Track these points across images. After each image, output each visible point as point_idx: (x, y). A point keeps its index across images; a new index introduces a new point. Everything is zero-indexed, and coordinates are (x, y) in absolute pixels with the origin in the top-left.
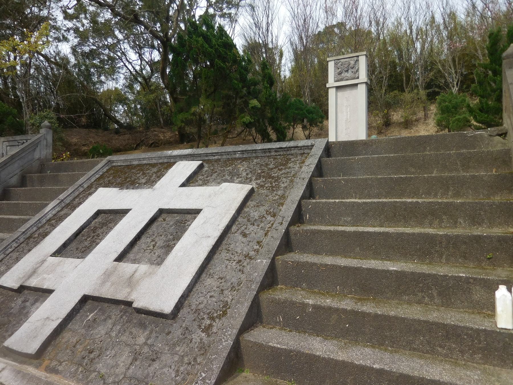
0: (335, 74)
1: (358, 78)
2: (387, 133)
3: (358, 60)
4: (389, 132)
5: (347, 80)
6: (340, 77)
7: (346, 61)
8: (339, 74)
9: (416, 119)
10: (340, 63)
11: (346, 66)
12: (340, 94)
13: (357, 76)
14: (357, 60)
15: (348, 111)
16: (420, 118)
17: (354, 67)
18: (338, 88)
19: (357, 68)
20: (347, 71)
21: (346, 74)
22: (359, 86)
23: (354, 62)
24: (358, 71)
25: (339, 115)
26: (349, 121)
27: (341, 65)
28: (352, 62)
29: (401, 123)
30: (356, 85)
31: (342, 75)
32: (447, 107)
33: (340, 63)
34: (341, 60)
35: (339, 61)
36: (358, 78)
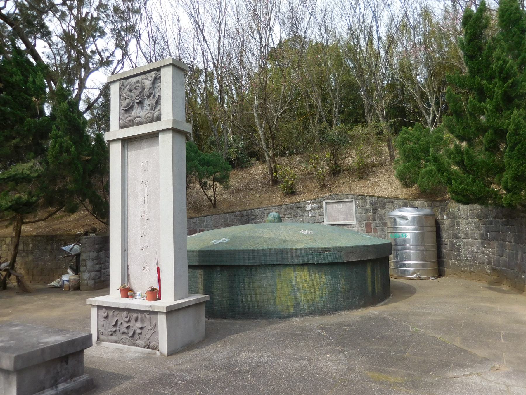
0: (120, 111)
1: (159, 119)
2: (334, 186)
3: (160, 78)
4: (337, 184)
5: (139, 123)
6: (129, 117)
7: (138, 82)
8: (126, 111)
9: (379, 162)
10: (128, 87)
11: (137, 92)
12: (132, 154)
13: (156, 115)
14: (157, 80)
15: (146, 195)
16: (385, 161)
17: (151, 94)
18: (126, 142)
19: (157, 95)
20: (141, 103)
21: (139, 109)
22: (161, 136)
23: (150, 82)
24: (158, 102)
25: (131, 202)
26: (146, 218)
27: (130, 91)
28: (148, 84)
29: (355, 170)
30: (153, 136)
31: (133, 112)
32: (412, 150)
33: (128, 87)
34: (130, 80)
35: (126, 82)
36: (159, 119)
